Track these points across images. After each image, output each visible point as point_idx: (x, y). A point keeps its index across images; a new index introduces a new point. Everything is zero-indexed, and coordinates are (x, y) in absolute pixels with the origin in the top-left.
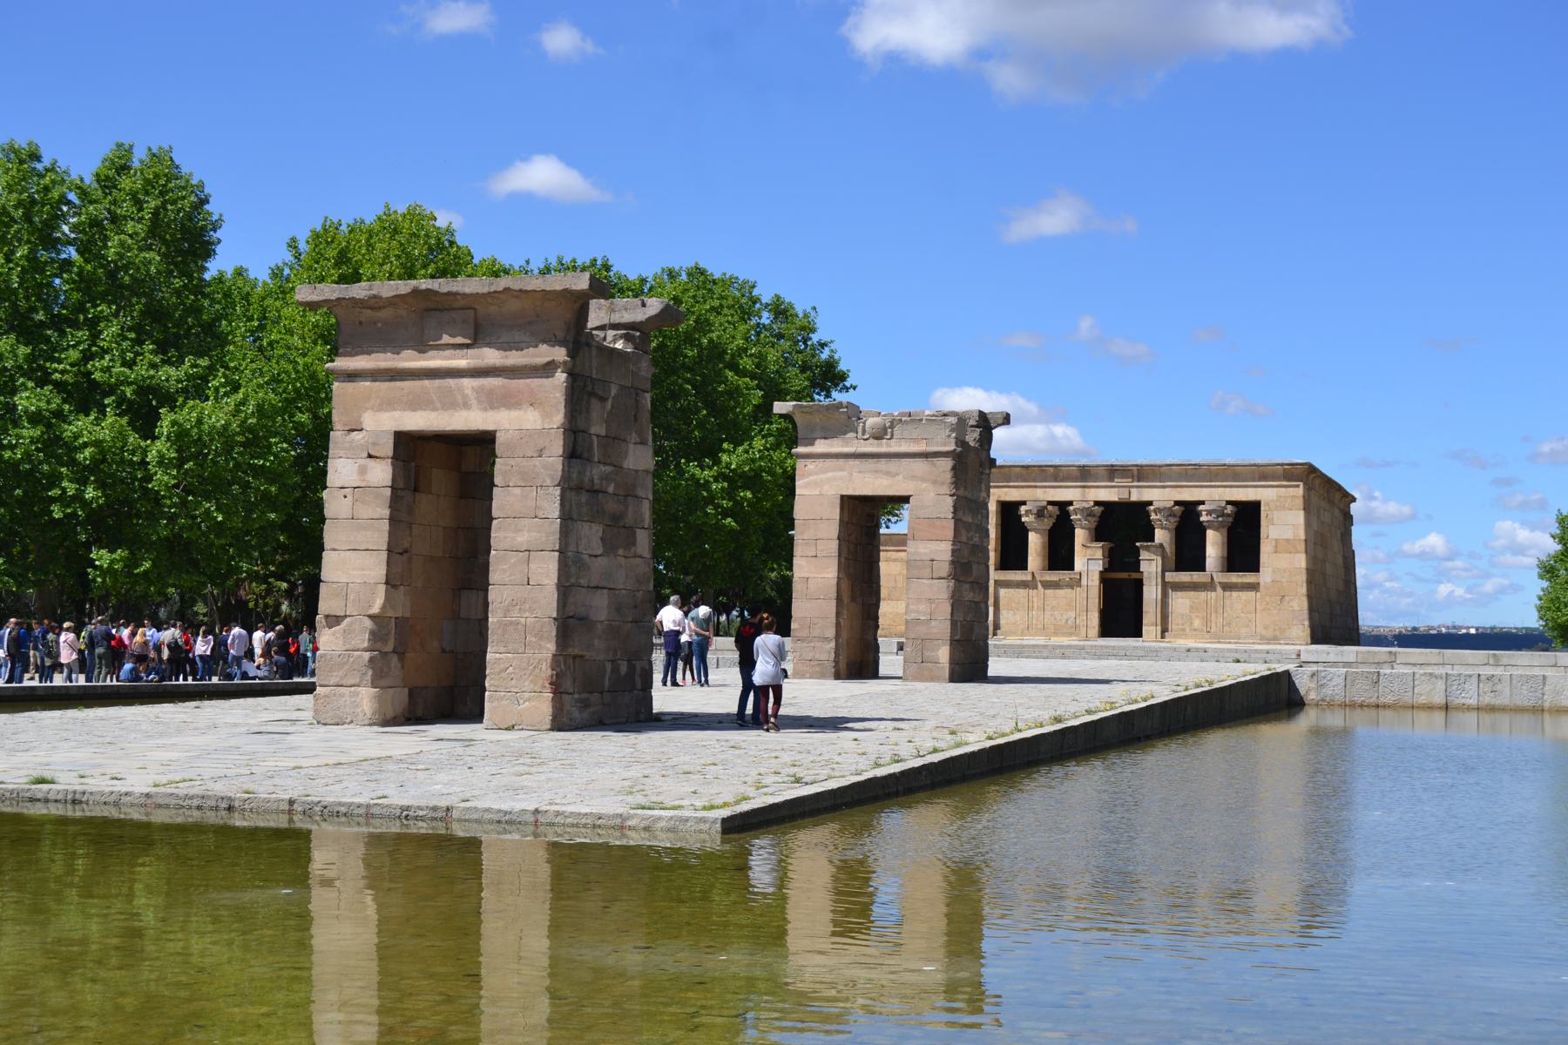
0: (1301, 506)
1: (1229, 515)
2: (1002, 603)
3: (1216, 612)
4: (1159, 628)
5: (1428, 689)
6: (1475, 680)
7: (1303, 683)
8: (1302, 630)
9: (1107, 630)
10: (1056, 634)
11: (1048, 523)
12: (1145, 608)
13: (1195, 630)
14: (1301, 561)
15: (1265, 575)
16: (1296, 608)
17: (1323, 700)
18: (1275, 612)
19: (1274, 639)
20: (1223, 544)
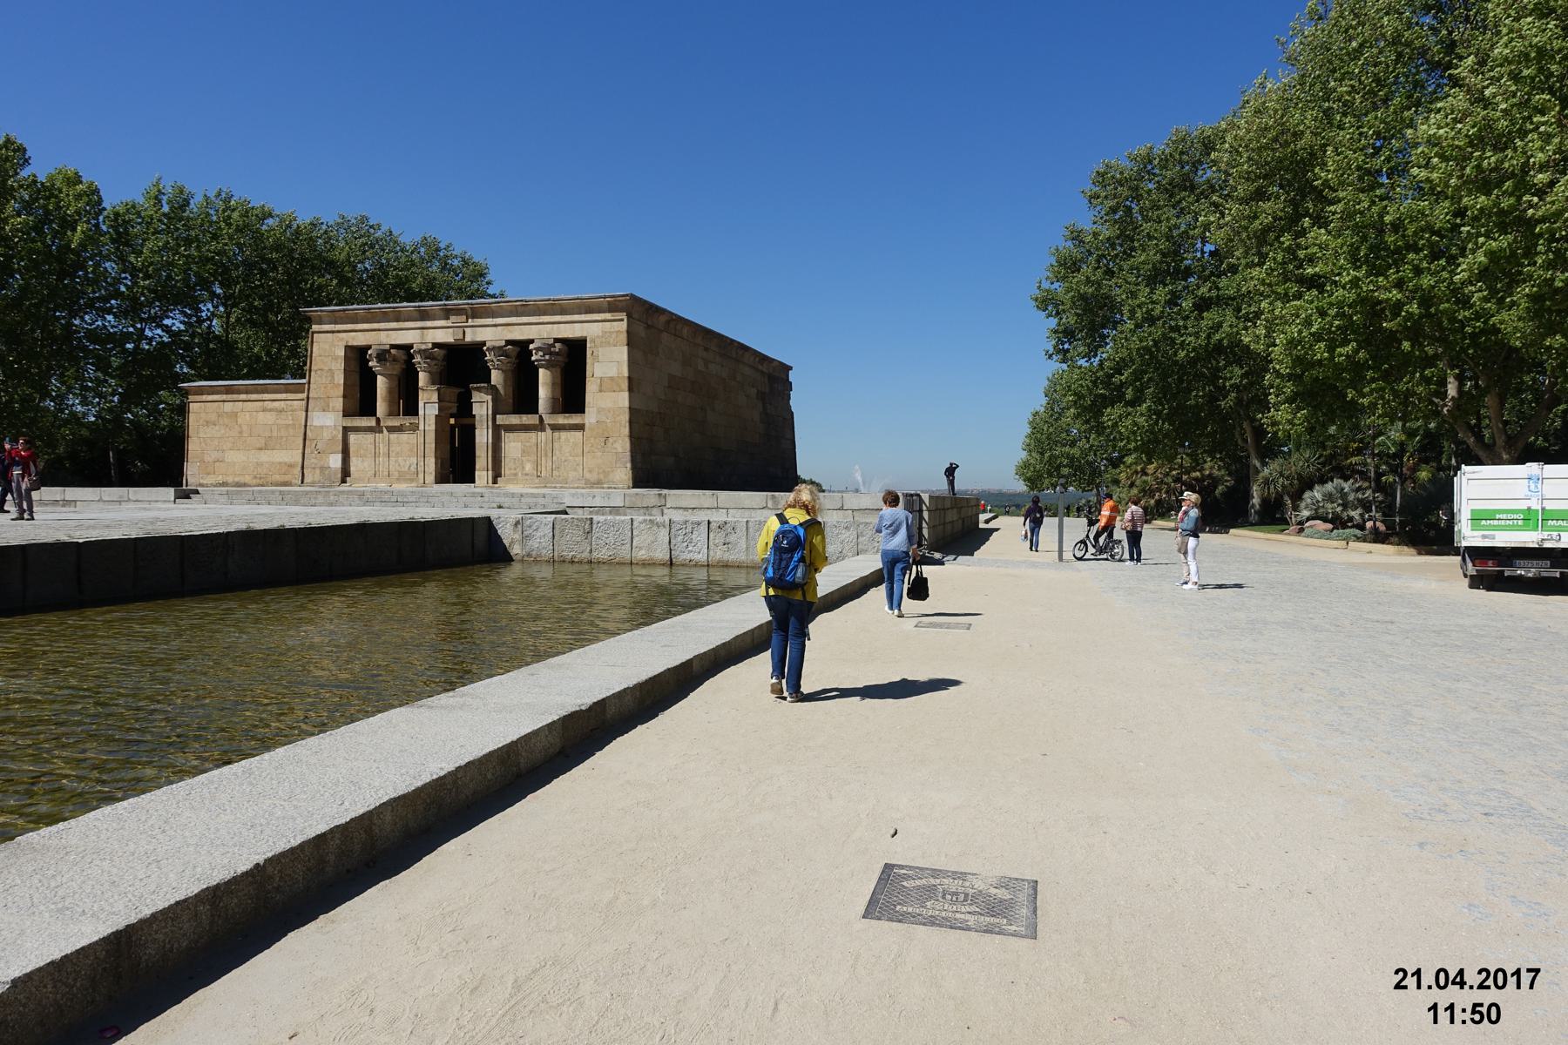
0: (625, 342)
1: (557, 354)
2: (352, 449)
3: (546, 455)
4: (490, 473)
5: (648, 541)
6: (704, 527)
7: (506, 533)
8: (624, 474)
9: (441, 479)
10: (398, 480)
11: (396, 369)
12: (478, 453)
13: (527, 475)
14: (623, 399)
15: (590, 417)
16: (620, 450)
17: (529, 555)
18: (600, 454)
19: (598, 484)
20: (553, 384)
